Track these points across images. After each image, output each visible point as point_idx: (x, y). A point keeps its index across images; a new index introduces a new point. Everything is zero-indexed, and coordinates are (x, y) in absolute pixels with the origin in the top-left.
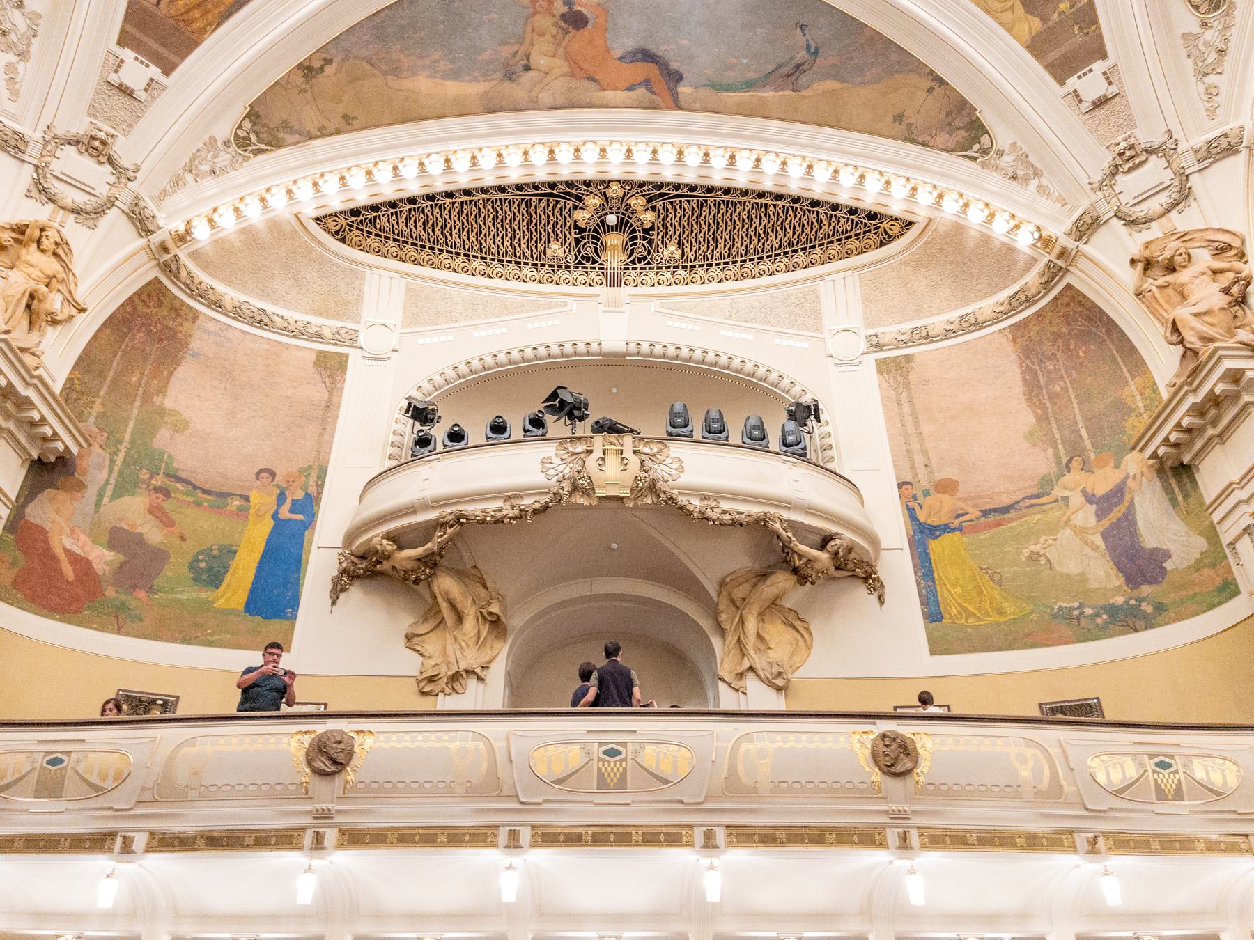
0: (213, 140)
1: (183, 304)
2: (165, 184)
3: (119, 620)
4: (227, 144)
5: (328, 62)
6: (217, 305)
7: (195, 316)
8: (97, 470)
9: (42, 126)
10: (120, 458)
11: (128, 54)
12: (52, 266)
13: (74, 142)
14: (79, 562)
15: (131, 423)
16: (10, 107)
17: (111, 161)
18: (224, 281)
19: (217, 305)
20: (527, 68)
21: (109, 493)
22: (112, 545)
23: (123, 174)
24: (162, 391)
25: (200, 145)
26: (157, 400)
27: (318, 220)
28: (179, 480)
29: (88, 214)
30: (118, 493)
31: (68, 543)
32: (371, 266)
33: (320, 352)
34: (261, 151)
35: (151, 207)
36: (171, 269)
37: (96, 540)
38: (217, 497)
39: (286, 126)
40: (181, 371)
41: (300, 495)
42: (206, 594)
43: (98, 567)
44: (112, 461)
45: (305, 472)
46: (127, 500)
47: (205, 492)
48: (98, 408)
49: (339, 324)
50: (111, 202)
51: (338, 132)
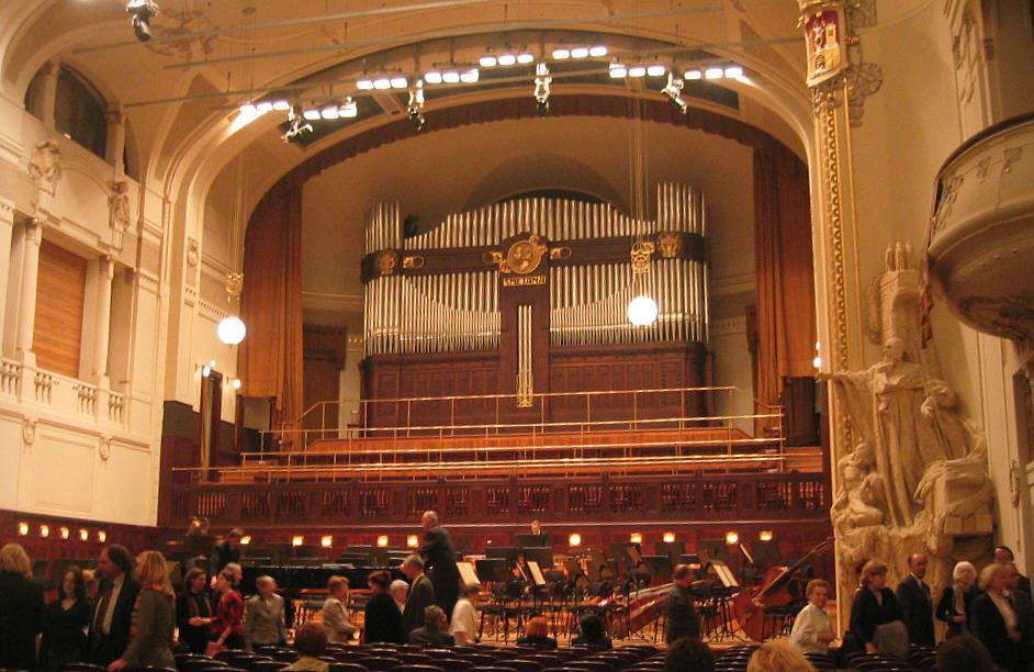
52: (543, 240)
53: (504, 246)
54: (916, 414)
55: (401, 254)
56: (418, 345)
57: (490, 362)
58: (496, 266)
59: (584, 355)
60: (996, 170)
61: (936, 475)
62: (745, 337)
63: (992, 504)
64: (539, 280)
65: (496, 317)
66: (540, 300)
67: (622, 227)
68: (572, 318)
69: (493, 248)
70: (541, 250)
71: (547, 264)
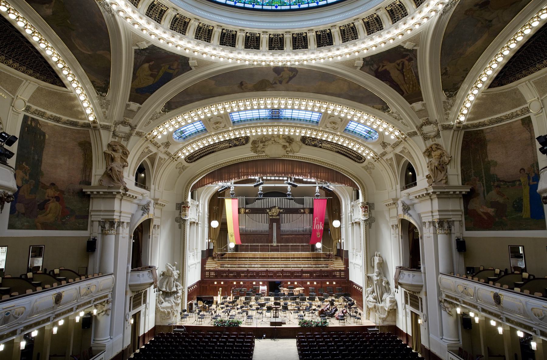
0: (444, 102)
1: (477, 130)
3: (502, 226)
4: (448, 99)
5: (446, 68)
7: (482, 130)
8: (480, 188)
9: (415, 128)
11: (414, 104)
12: (438, 152)
13: (422, 126)
14: (486, 214)
15: (483, 171)
16: (409, 128)
17: (431, 123)
18: (482, 118)
19: (484, 124)
20: (491, 21)
21: (486, 193)
22: (492, 207)
23: (436, 123)
24: (487, 156)
25: (443, 105)
26: (486, 160)
28: (501, 181)
29: (438, 135)
30: (488, 192)
31: (482, 210)
32: (517, 85)
33: (522, 119)
34: (457, 93)
35: (446, 123)
36: (466, 127)
38: (512, 183)
39: (455, 85)
40: (489, 147)
41: (533, 175)
42: (519, 214)
43: (492, 214)
44: (483, 184)
45: (532, 166)
47: (509, 182)
48: (473, 171)
49: (521, 107)
50: (438, 131)
51: (467, 74)
52: (279, 208)
53: (270, 209)
54: (382, 285)
55: (246, 209)
56: (250, 231)
57: (268, 237)
58: (268, 213)
59: (288, 235)
61: (387, 297)
63: (396, 304)
64: (278, 217)
65: (268, 225)
66: (277, 221)
67: (298, 206)
68: (286, 227)
70: (278, 210)
71: (280, 213)
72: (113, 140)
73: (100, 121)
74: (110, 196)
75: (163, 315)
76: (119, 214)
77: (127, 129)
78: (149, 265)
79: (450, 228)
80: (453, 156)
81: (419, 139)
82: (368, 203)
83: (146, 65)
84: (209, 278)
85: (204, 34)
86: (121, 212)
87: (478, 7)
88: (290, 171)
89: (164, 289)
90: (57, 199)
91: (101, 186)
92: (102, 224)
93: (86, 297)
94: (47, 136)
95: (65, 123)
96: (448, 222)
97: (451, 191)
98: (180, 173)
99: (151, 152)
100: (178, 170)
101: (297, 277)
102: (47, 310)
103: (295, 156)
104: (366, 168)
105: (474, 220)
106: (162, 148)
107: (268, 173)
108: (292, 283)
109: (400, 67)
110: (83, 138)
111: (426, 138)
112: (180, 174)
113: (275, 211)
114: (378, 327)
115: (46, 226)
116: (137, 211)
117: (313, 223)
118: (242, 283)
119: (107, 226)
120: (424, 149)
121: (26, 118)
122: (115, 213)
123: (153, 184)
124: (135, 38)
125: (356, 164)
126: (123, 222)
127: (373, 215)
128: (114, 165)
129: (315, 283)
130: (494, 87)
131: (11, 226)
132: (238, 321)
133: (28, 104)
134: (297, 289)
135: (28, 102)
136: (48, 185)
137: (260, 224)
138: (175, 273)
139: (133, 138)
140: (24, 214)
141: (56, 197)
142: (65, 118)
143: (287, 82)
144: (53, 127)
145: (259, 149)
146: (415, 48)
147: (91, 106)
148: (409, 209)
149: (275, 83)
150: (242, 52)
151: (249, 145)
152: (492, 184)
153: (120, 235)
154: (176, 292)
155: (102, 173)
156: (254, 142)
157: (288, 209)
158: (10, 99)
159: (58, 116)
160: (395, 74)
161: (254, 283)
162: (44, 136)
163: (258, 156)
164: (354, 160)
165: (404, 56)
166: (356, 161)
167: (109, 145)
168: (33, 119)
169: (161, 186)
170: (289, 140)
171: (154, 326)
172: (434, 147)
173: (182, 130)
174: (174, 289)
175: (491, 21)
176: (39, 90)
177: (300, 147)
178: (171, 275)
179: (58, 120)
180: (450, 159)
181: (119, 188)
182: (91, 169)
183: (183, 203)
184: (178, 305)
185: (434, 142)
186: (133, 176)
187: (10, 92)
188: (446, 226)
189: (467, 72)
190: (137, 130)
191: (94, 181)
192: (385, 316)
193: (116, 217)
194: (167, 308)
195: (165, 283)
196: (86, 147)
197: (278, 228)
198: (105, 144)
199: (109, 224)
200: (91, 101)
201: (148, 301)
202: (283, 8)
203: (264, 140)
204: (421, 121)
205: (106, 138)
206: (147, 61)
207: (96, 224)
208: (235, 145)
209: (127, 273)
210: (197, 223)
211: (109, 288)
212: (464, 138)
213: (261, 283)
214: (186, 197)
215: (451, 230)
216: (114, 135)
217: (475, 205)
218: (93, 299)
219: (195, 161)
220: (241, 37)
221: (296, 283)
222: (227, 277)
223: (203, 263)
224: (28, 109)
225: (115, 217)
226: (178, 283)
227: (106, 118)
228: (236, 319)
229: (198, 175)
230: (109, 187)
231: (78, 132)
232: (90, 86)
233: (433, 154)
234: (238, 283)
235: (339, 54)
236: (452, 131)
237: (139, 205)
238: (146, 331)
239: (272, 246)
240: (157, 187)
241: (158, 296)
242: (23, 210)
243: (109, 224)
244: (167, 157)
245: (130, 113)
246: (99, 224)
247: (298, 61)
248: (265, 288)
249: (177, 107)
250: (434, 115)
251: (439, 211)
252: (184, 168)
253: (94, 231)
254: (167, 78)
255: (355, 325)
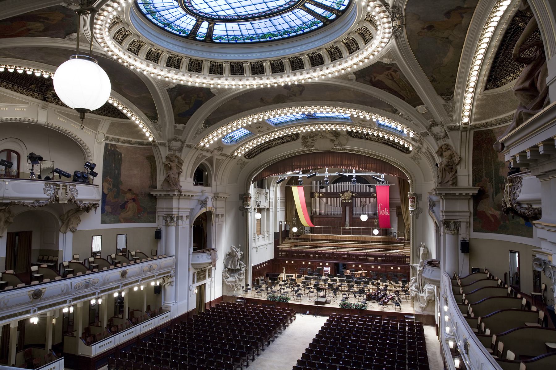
0: (444, 105)
2: (449, 119)
5: (432, 76)
6: (492, 125)
7: (491, 130)
8: (490, 190)
10: (494, 184)
12: (449, 152)
14: (493, 216)
17: (438, 125)
19: (492, 125)
20: (447, 38)
26: (497, 161)
27: (486, 89)
29: (446, 136)
30: (496, 194)
31: (490, 212)
36: (473, 128)
37: (496, 210)
43: (498, 217)
46: (499, 194)
48: (484, 172)
53: (343, 193)
57: (340, 220)
60: (430, 271)
62: (395, 213)
64: (350, 201)
65: (341, 208)
66: (350, 205)
67: (370, 190)
69: (340, 193)
71: (352, 197)
72: (170, 153)
73: (158, 140)
74: (169, 197)
75: (228, 287)
76: (177, 210)
77: (179, 144)
78: (213, 247)
79: (457, 228)
80: (463, 156)
81: (431, 138)
82: (415, 194)
83: (179, 98)
84: (281, 257)
85: (216, 69)
86: (179, 209)
87: (425, 30)
88: (340, 163)
89: (229, 267)
90: (134, 200)
91: (162, 189)
92: (165, 218)
93: (149, 273)
94: (123, 155)
95: (134, 144)
96: (455, 223)
97: (457, 192)
98: (242, 168)
99: (206, 157)
100: (240, 166)
101: (361, 260)
102: (116, 281)
103: (342, 149)
104: (414, 158)
105: (483, 222)
106: (215, 152)
107: (319, 165)
108: (357, 266)
109: (390, 77)
110: (148, 152)
111: (437, 138)
112: (242, 169)
113: (347, 195)
114: (416, 315)
115: (127, 221)
116: (196, 206)
117: (379, 209)
118: (309, 263)
119: (169, 220)
120: (437, 149)
121: (106, 145)
122: (174, 210)
123: (215, 181)
124: (163, 83)
125: (404, 154)
126: (182, 216)
127: (421, 206)
128: (171, 173)
129: (379, 267)
130: (492, 88)
131: (103, 222)
132: (287, 298)
133: (106, 135)
134: (360, 272)
135: (107, 133)
136: (127, 190)
137: (332, 207)
138: (239, 254)
139: (185, 150)
140: (111, 213)
141: (132, 199)
142: (134, 140)
143: (300, 94)
144: (127, 148)
145: (309, 143)
146: (393, 62)
147: (149, 130)
148: (434, 205)
149: (290, 96)
150: (250, 78)
151: (300, 140)
152: (500, 186)
153: (180, 227)
154: (240, 270)
155: (163, 179)
156: (304, 138)
157: (360, 193)
158: (94, 134)
159: (129, 139)
160: (388, 83)
161: (321, 264)
162: (121, 155)
163: (308, 150)
164: (401, 151)
165: (389, 69)
166: (403, 152)
167: (167, 158)
168: (112, 145)
169: (222, 181)
170: (336, 134)
171: (221, 295)
172: (443, 147)
173: (230, 135)
174: (238, 267)
175: (447, 38)
176: (112, 125)
177: (348, 140)
178: (235, 256)
179: (129, 142)
180: (459, 159)
181: (174, 191)
182: (156, 176)
183: (245, 194)
184: (242, 280)
185: (445, 143)
186: (191, 177)
187: (94, 130)
188: (452, 226)
189: (454, 77)
190: (186, 144)
191: (159, 186)
192: (424, 306)
193: (175, 213)
194: (231, 282)
195: (230, 262)
196: (151, 160)
197: (351, 212)
198: (164, 156)
199: (170, 219)
200: (148, 127)
201: (213, 275)
202: (276, 38)
203: (313, 135)
204: (429, 123)
205: (164, 152)
206: (180, 94)
207: (161, 218)
208: (288, 141)
209: (189, 254)
210: (268, 209)
211: (171, 266)
212: (474, 137)
213: (327, 264)
214: (248, 188)
215: (458, 231)
216: (170, 149)
217: (484, 206)
218: (157, 274)
219: (253, 157)
220: (247, 66)
221: (360, 266)
222: (299, 257)
223: (277, 243)
224: (107, 138)
225: (173, 213)
226: (242, 262)
227: (161, 137)
228: (287, 295)
229: (257, 169)
230: (167, 191)
231: (145, 149)
232: (144, 117)
233: (444, 154)
234: (307, 263)
235: (329, 72)
236: (460, 132)
237: (198, 201)
238: (213, 299)
239: (344, 229)
240: (219, 183)
241: (224, 272)
242: (110, 210)
243: (170, 219)
244: (224, 158)
245: (178, 132)
246: (163, 219)
247: (297, 81)
248: (329, 269)
249: (215, 123)
250: (439, 118)
251: (445, 212)
252: (244, 164)
253: (159, 224)
254: (198, 104)
255: (394, 311)
